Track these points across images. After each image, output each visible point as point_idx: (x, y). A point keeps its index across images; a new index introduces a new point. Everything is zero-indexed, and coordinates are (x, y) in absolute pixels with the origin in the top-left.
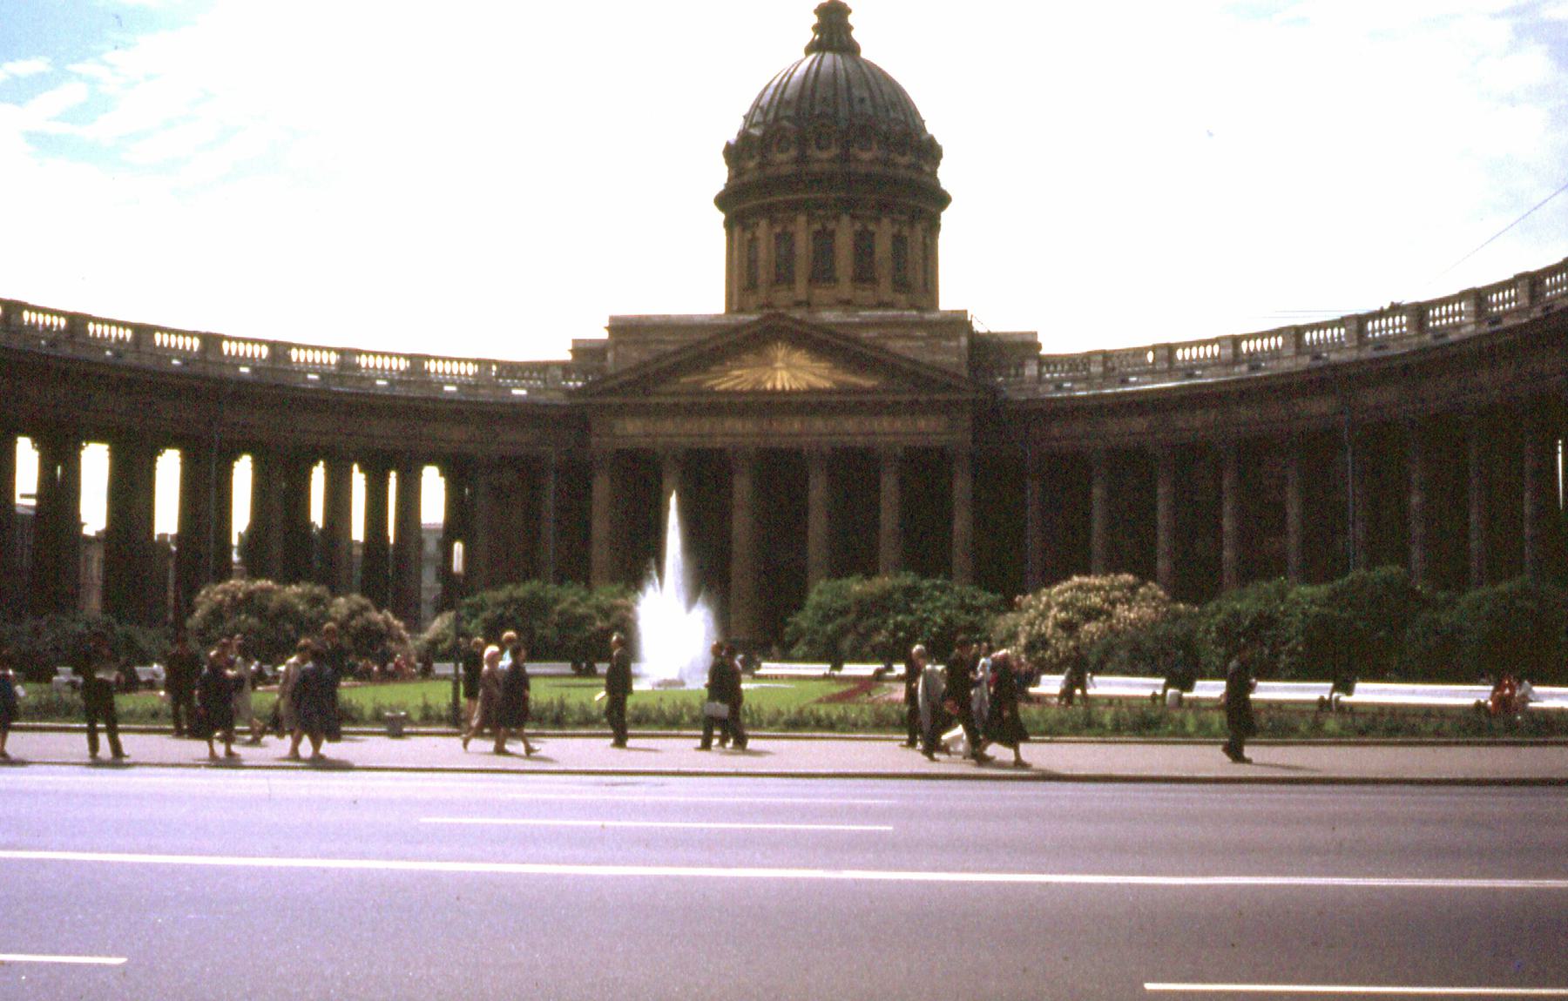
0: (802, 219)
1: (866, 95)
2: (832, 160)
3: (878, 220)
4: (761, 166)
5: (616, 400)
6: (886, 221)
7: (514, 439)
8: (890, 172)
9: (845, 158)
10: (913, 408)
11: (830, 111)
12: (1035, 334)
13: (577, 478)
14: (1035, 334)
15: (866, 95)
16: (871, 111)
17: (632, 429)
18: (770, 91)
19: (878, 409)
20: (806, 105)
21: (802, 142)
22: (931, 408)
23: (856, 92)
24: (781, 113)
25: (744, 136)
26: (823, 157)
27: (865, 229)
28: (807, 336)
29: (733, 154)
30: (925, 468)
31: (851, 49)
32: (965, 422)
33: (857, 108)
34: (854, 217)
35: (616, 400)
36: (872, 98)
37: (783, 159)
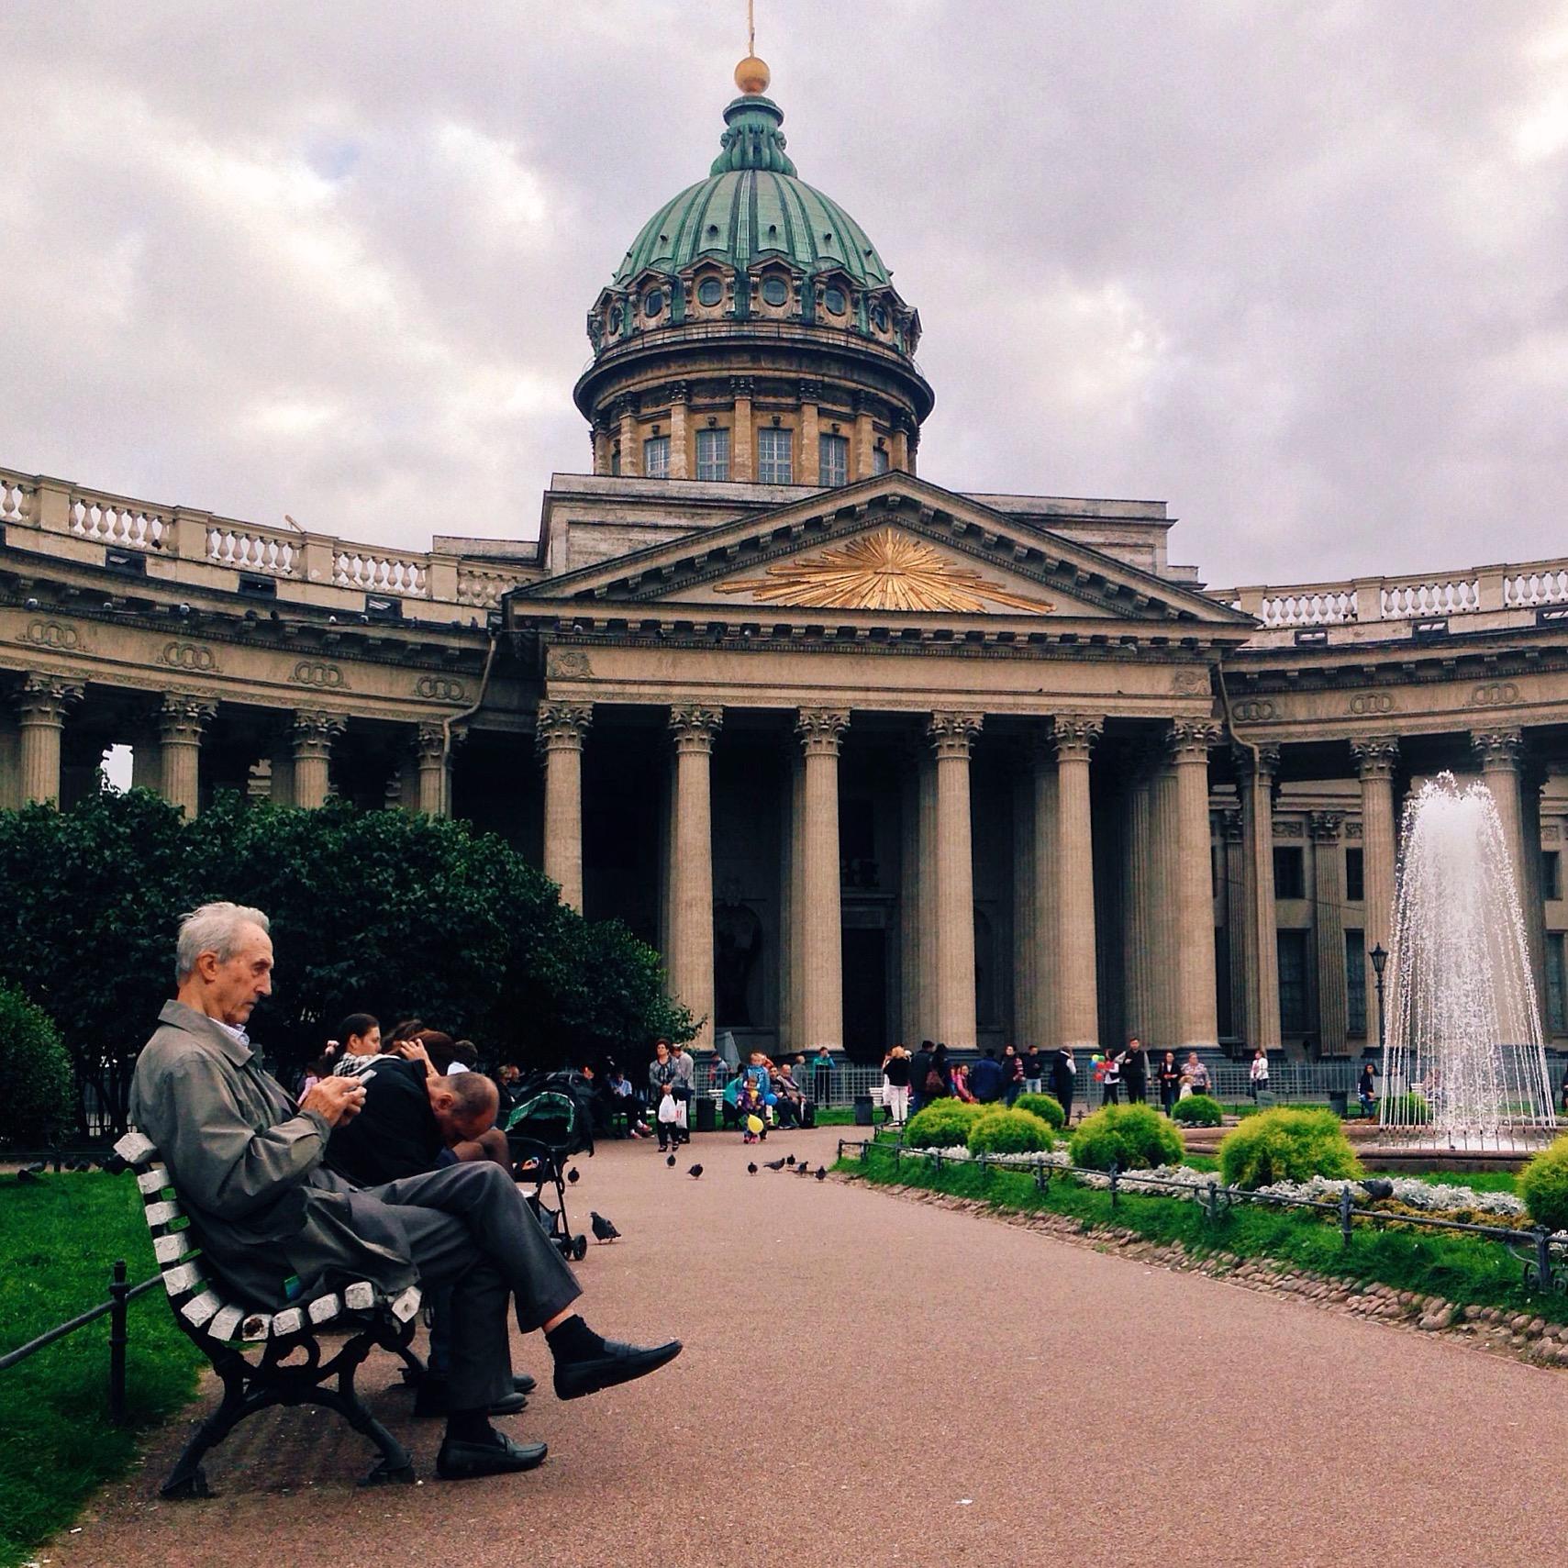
0: (743, 408)
1: (832, 231)
2: (789, 322)
3: (852, 420)
4: (673, 325)
5: (601, 615)
6: (866, 425)
8: (873, 348)
9: (809, 324)
11: (783, 247)
15: (832, 231)
17: (626, 676)
18: (677, 216)
20: (743, 235)
21: (743, 286)
22: (1158, 653)
23: (821, 228)
24: (704, 246)
26: (777, 309)
29: (608, 309)
32: (1203, 685)
34: (821, 413)
35: (601, 615)
36: (843, 245)
37: (712, 313)
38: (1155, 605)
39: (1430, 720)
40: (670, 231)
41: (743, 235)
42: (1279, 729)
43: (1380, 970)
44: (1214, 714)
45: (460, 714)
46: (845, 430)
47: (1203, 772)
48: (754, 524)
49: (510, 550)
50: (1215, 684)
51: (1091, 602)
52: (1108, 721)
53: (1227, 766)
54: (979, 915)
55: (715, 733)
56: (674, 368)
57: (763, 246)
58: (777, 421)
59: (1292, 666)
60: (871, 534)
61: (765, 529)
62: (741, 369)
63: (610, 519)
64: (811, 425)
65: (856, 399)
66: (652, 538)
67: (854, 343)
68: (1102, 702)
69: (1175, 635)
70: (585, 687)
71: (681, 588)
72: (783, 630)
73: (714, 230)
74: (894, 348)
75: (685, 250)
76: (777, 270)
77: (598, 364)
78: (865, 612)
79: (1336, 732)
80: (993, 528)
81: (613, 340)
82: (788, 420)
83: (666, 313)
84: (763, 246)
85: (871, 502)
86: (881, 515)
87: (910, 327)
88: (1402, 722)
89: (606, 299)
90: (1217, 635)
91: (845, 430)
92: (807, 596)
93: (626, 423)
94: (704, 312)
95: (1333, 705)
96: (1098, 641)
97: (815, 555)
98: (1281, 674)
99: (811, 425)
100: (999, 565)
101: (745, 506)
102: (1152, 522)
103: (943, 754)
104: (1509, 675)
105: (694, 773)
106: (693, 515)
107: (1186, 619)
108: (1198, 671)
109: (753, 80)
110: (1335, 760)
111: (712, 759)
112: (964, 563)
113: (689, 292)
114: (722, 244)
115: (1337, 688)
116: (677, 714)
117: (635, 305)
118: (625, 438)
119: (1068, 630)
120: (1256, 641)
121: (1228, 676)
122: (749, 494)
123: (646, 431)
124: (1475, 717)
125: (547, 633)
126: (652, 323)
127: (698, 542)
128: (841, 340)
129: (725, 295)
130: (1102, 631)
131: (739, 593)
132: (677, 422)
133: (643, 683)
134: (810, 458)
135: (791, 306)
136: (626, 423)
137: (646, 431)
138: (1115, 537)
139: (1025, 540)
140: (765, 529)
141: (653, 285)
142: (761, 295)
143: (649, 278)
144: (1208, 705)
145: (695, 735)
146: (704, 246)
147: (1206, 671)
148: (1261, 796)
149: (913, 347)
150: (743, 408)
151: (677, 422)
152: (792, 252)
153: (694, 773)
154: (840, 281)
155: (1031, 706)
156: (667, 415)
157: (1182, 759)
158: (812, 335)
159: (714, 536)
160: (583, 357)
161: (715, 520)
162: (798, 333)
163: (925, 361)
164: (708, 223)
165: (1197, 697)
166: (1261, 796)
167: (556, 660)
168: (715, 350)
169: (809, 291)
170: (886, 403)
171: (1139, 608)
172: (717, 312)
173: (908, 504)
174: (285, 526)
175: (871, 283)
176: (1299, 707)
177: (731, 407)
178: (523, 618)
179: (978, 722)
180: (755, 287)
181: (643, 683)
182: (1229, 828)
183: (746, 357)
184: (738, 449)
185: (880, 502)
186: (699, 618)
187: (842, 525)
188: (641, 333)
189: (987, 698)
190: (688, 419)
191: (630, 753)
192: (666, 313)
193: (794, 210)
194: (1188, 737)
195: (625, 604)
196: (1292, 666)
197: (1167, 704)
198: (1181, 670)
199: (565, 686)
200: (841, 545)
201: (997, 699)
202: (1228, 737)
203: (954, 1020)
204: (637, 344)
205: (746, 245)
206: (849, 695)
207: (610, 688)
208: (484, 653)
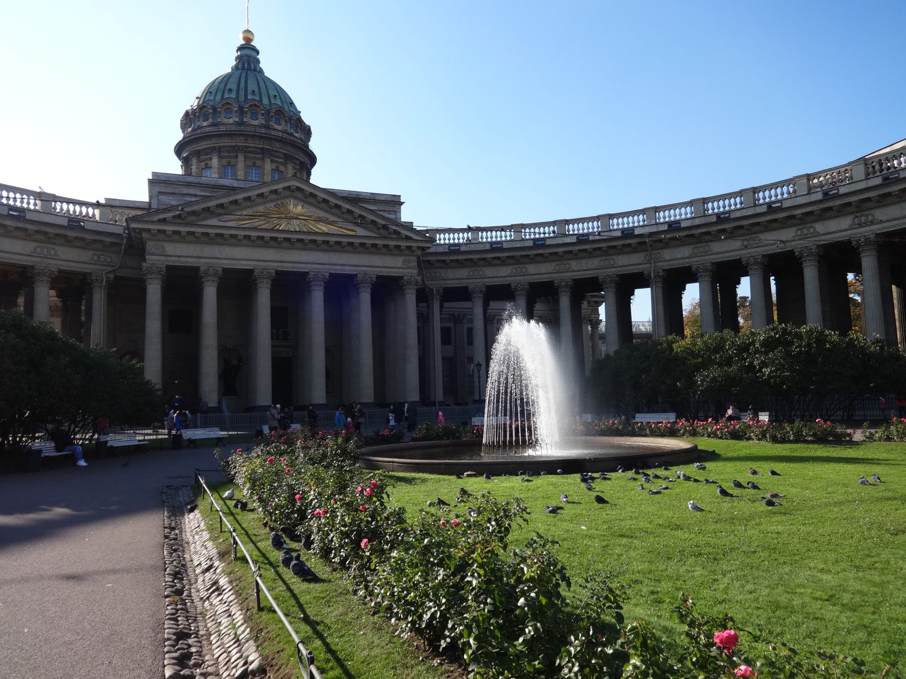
0: (241, 158)
2: (260, 126)
3: (285, 164)
4: (213, 125)
5: (170, 228)
7: (71, 259)
9: (268, 127)
10: (387, 250)
11: (257, 98)
12: (412, 223)
13: (126, 293)
14: (412, 223)
16: (279, 103)
17: (182, 254)
19: (363, 248)
20: (242, 93)
23: (272, 93)
24: (226, 96)
25: (201, 108)
27: (277, 169)
28: (312, 195)
29: (188, 119)
30: (386, 289)
31: (261, 71)
32: (414, 264)
33: (273, 101)
34: (272, 161)
35: (170, 228)
38: (395, 232)
39: (496, 279)
40: (213, 90)
41: (242, 93)
42: (443, 282)
43: (479, 371)
44: (418, 275)
45: (110, 269)
46: (282, 168)
47: (414, 296)
48: (235, 194)
49: (137, 205)
50: (419, 265)
51: (372, 231)
52: (378, 277)
53: (423, 296)
54: (327, 350)
55: (220, 279)
56: (213, 141)
57: (250, 97)
58: (254, 163)
59: (446, 258)
60: (284, 201)
61: (240, 196)
62: (240, 142)
63: (176, 191)
64: (268, 166)
65: (287, 157)
66: (193, 199)
67: (285, 136)
68: (376, 269)
69: (404, 244)
70: (163, 258)
71: (205, 219)
72: (247, 237)
73: (230, 90)
74: (301, 139)
75: (219, 97)
76: (255, 107)
77: (184, 138)
78: (283, 231)
79: (463, 283)
80: (333, 200)
81: (190, 130)
82: (259, 163)
83: (211, 120)
84: (250, 97)
85: (284, 188)
86: (288, 193)
87: (307, 132)
88: (487, 280)
89: (187, 114)
90: (420, 245)
91: (282, 168)
92: (258, 224)
93: (194, 161)
94: (226, 121)
95: (463, 273)
96: (374, 246)
97: (261, 208)
98: (444, 261)
99: (268, 166)
100: (337, 216)
101: (233, 189)
102: (395, 202)
103: (313, 288)
104: (524, 263)
105: (210, 293)
106: (212, 192)
107: (408, 238)
108: (412, 258)
109: (248, 37)
110: (462, 294)
111: (218, 289)
112: (322, 214)
113: (220, 112)
114: (233, 95)
115: (464, 267)
116: (202, 269)
117: (199, 117)
118: (194, 168)
119: (363, 241)
120: (433, 250)
121: (424, 261)
122: (235, 184)
123: (203, 165)
124: (512, 278)
125: (144, 235)
126: (205, 124)
127: (211, 200)
128: (280, 134)
129: (234, 115)
130: (376, 242)
131: (231, 223)
132: (215, 162)
133: (188, 257)
134: (267, 178)
135: (261, 121)
136: (194, 161)
137: (203, 165)
138: (381, 208)
139: (346, 206)
140: (240, 196)
141: (205, 109)
142: (249, 115)
143: (204, 107)
144: (416, 271)
145: (210, 278)
146: (226, 96)
147: (415, 258)
148: (436, 305)
149: (309, 140)
150: (241, 158)
151: (215, 162)
152: (261, 100)
153: (210, 293)
154: (280, 112)
155: (348, 270)
156: (211, 159)
157: (407, 291)
158: (268, 132)
159: (217, 199)
160: (179, 136)
161: (222, 192)
162: (263, 131)
163: (314, 145)
164: (228, 87)
165: (412, 268)
166: (436, 305)
167: (150, 246)
168: (230, 135)
169: (267, 114)
170: (297, 159)
171: (390, 233)
172: (231, 121)
173: (298, 189)
174: (39, 190)
175: (292, 114)
176: (450, 273)
177: (237, 157)
178: (134, 229)
179: (327, 275)
180: (246, 112)
181: (188, 257)
182: (423, 319)
183: (242, 138)
184: (239, 173)
185: (289, 187)
186: (212, 231)
187: (274, 196)
188: (200, 127)
189: (331, 267)
190: (219, 161)
191: (183, 285)
192: (211, 120)
193: (262, 85)
194: (409, 283)
195: (180, 224)
196: (446, 258)
197: (401, 270)
198: (407, 258)
199: (153, 257)
200: (272, 204)
201: (334, 267)
202: (424, 284)
203: (318, 394)
204: (199, 131)
205: (243, 97)
206: (276, 264)
207: (174, 259)
208: (120, 245)
